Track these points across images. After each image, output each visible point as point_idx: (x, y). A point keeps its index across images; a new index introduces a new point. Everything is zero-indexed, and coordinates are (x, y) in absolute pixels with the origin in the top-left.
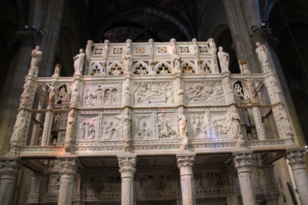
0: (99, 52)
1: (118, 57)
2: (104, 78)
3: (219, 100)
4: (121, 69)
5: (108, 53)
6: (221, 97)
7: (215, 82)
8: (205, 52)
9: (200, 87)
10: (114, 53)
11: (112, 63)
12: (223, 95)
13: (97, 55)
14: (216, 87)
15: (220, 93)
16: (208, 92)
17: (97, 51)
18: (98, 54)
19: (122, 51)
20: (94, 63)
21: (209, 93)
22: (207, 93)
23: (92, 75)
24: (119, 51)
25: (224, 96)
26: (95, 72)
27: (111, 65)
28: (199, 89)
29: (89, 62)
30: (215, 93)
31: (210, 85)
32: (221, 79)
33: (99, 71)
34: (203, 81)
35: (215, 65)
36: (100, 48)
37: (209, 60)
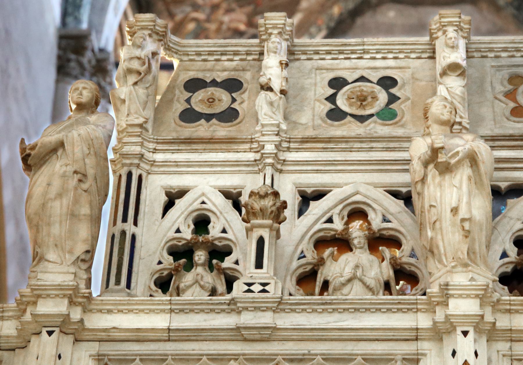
0: (218, 109)
1: (371, 149)
2: (266, 319)
4: (394, 242)
5: (286, 118)
10: (336, 115)
11: (319, 195)
13: (202, 129)
17: (201, 95)
18: (209, 117)
19: (393, 99)
20: (182, 193)
23: (163, 284)
24: (375, 98)
26: (190, 266)
27: (316, 208)
29: (140, 178)
33: (219, 252)
36: (220, 77)
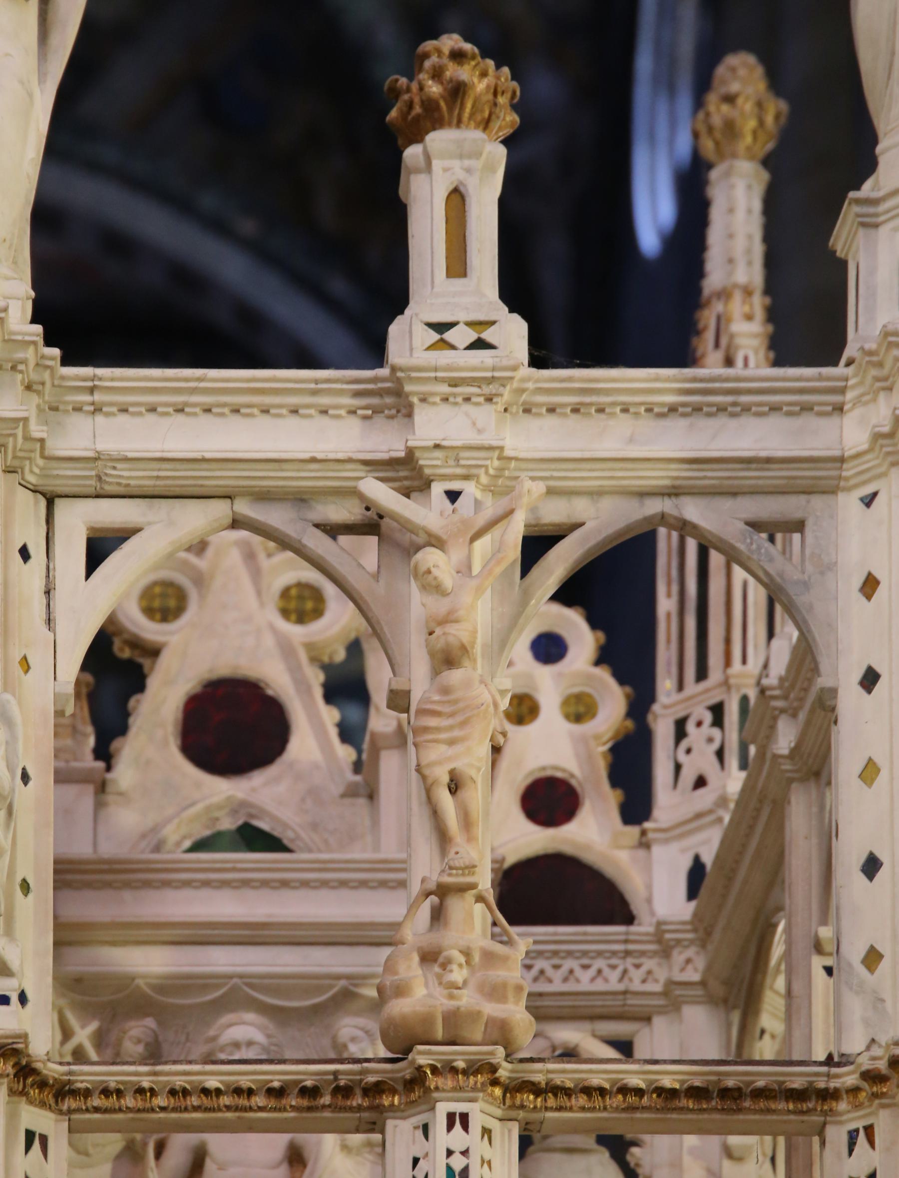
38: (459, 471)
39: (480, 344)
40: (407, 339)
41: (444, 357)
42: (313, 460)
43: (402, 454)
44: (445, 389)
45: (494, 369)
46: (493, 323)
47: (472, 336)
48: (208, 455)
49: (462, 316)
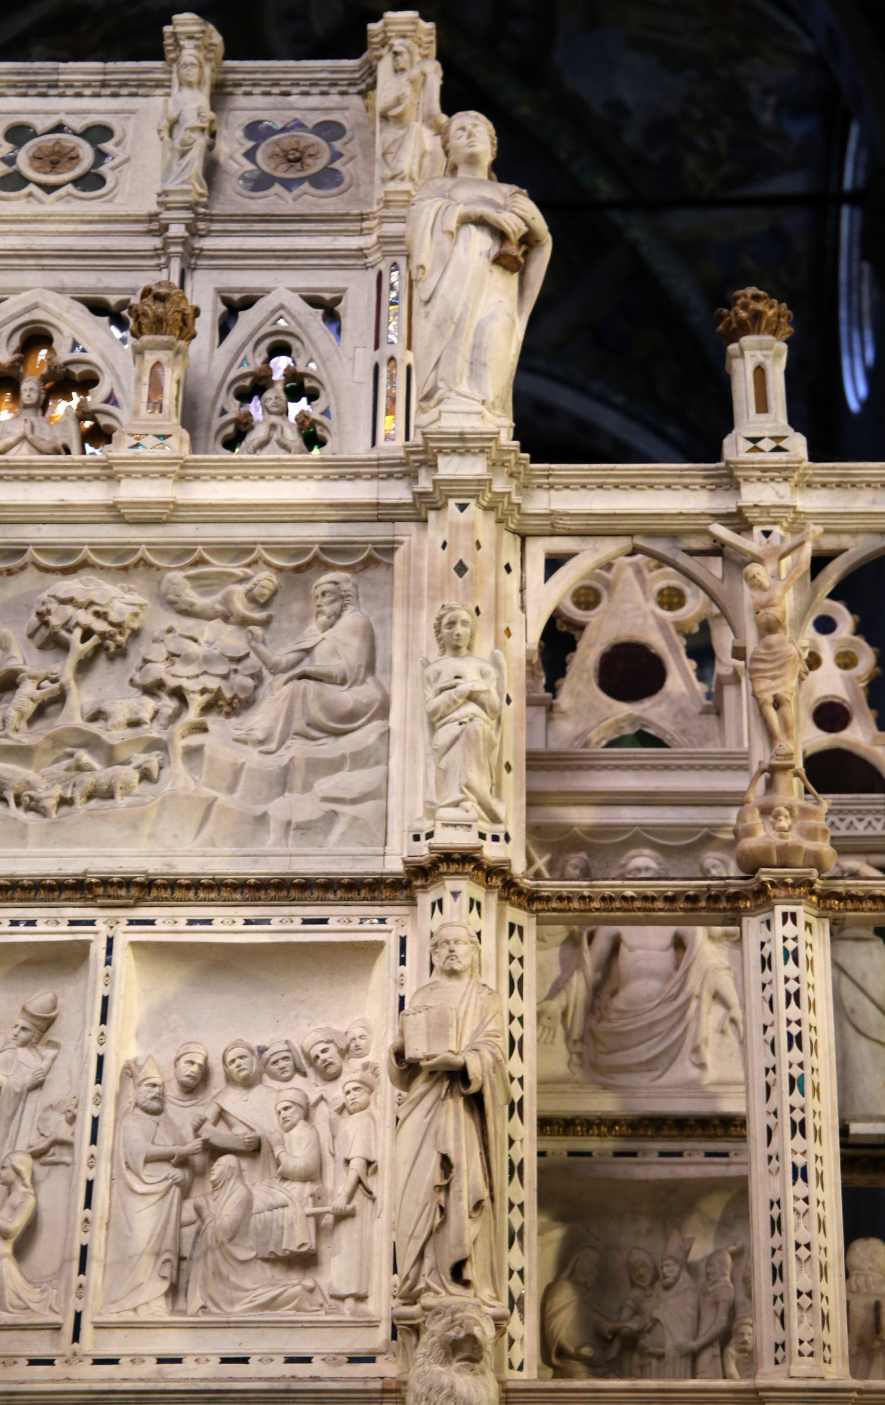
3: (303, 806)
6: (334, 766)
7: (298, 569)
8: (306, 186)
9: (87, 634)
12: (365, 736)
14: (312, 634)
15: (326, 708)
16: (179, 694)
21: (197, 701)
22: (169, 705)
25: (375, 756)
28: (79, 648)
30: (260, 719)
31: (241, 606)
32: (380, 532)
34: (162, 551)
35: (376, 356)
37: (322, 281)
38: (770, 520)
39: (778, 449)
40: (734, 447)
41: (757, 456)
42: (681, 514)
43: (734, 510)
44: (758, 474)
45: (788, 462)
46: (785, 438)
47: (773, 444)
48: (617, 512)
49: (766, 434)
